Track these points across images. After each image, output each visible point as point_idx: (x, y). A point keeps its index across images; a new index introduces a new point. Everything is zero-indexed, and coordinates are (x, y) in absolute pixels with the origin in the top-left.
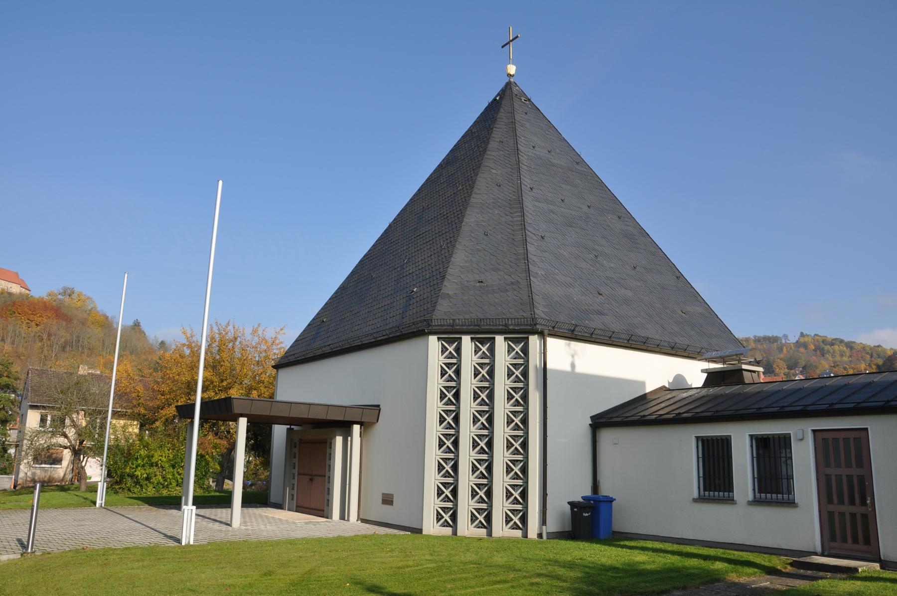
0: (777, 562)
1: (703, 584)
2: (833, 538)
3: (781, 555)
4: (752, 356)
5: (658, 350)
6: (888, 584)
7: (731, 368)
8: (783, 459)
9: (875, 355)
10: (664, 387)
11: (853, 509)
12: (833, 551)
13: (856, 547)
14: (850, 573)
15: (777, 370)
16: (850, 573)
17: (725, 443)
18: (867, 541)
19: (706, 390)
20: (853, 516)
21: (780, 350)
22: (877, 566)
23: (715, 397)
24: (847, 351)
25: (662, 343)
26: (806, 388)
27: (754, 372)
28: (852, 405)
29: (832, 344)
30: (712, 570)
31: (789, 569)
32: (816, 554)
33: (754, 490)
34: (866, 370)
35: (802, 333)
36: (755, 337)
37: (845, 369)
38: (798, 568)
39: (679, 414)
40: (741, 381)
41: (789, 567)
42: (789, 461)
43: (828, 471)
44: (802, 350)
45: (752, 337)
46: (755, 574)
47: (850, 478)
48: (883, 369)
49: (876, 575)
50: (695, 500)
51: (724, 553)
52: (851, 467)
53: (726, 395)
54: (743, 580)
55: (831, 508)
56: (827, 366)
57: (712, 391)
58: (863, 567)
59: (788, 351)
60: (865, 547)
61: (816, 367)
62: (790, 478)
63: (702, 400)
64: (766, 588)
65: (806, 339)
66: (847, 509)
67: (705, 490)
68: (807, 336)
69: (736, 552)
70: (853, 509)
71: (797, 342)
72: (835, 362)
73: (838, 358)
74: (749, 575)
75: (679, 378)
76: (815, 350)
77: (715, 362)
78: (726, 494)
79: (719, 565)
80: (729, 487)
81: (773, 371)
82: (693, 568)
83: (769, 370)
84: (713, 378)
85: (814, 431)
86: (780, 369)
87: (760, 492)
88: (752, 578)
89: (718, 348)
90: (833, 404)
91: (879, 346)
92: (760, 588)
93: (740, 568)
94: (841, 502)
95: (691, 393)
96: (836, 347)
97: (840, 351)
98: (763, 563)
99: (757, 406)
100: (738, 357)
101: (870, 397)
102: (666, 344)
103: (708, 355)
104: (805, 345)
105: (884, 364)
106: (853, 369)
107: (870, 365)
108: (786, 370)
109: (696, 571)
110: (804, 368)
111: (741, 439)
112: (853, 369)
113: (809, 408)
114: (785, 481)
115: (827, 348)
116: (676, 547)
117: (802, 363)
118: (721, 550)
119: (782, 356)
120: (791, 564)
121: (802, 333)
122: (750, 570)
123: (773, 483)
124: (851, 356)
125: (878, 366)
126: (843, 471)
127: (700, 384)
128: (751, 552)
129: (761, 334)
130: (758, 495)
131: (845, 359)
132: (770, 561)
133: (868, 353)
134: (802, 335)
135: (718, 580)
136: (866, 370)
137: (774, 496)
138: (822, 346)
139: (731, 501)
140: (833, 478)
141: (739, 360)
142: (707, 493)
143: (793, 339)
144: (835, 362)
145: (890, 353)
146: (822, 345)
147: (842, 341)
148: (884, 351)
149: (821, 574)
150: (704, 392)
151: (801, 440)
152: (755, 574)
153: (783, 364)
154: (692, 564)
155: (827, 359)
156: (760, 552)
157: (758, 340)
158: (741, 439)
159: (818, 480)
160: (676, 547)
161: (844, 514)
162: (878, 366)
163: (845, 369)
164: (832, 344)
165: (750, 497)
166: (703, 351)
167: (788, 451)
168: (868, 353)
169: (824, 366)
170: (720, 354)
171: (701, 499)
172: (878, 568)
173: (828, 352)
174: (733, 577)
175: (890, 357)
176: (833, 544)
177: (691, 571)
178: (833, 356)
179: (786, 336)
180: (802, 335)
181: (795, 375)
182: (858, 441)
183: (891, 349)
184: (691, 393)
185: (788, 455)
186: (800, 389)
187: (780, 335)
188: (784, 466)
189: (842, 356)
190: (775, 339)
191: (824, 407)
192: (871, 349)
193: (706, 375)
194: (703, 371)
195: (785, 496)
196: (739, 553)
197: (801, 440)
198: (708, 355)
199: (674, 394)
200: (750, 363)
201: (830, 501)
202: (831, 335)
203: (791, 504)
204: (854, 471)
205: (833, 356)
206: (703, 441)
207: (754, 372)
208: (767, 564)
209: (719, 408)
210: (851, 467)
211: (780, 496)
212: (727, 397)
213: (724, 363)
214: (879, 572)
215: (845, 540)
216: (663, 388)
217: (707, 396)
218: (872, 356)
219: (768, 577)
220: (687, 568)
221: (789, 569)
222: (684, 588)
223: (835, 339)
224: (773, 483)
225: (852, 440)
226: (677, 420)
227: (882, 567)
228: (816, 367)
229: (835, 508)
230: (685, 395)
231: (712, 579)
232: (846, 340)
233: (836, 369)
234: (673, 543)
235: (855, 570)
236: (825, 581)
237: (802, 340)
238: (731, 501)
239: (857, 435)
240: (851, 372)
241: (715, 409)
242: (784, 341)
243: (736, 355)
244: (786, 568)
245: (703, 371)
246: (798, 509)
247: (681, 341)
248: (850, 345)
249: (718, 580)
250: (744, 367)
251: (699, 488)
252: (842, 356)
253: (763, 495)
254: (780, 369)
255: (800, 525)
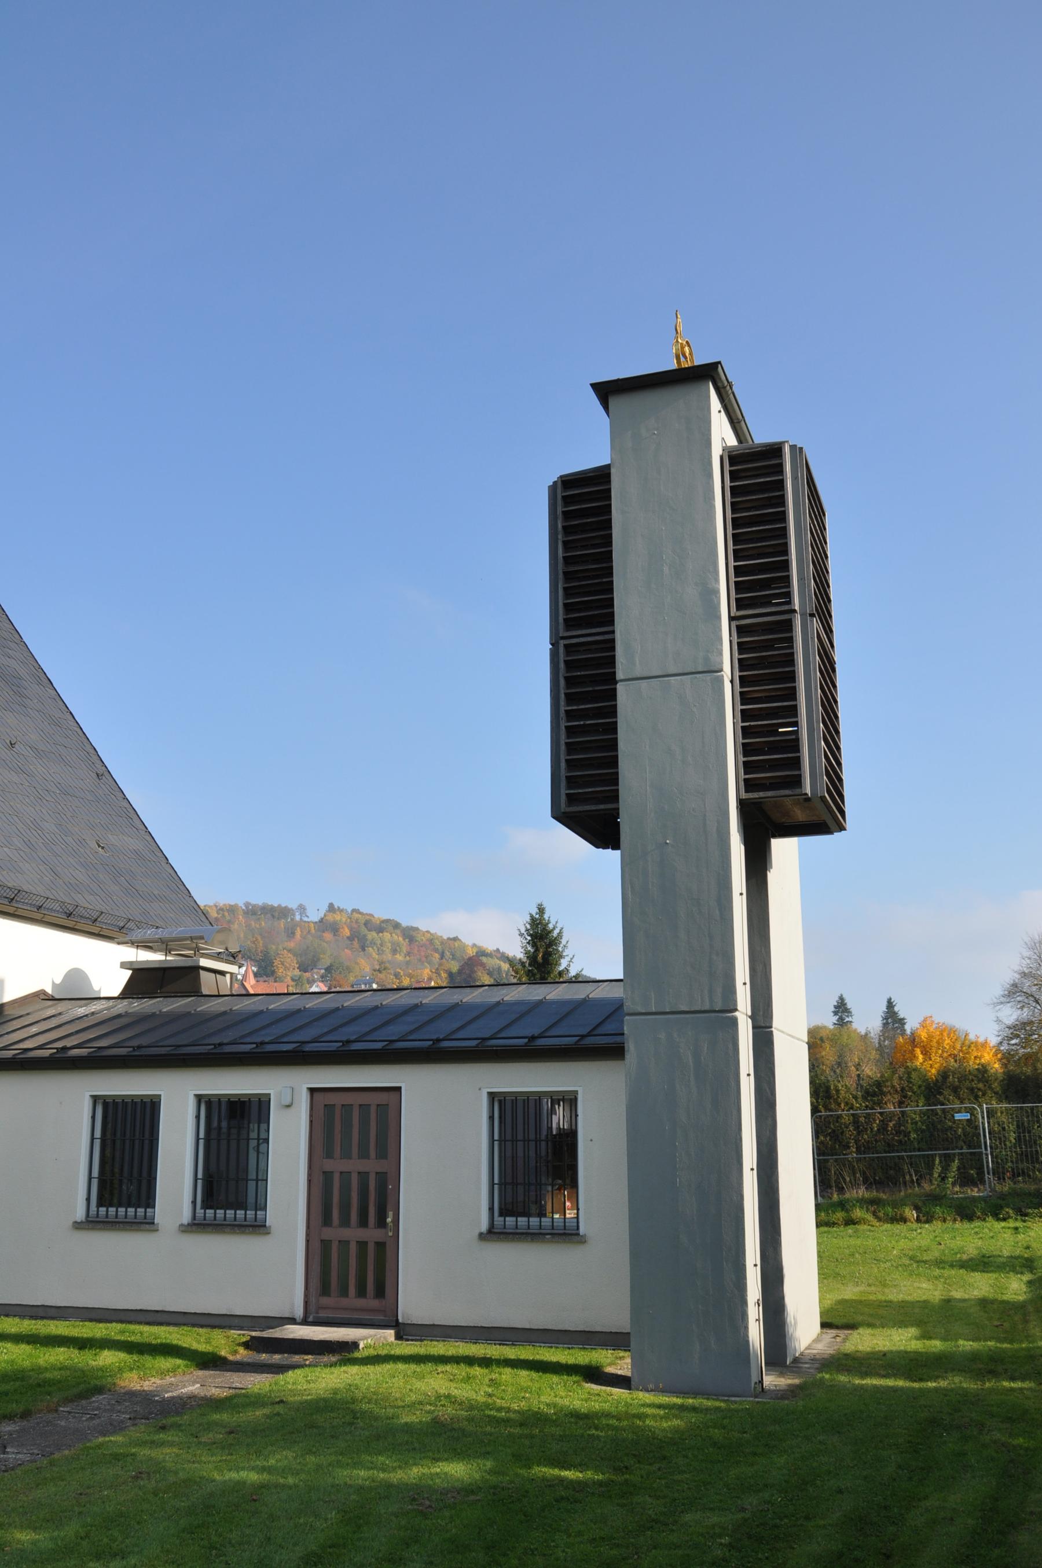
0: (222, 1343)
1: (67, 1401)
2: (325, 1290)
3: (230, 1327)
4: (222, 943)
5: (38, 916)
6: (401, 1366)
7: (181, 962)
8: (253, 1144)
9: (448, 954)
10: (43, 992)
11: (362, 1234)
12: (323, 1314)
13: (361, 1302)
14: (344, 1351)
15: (280, 972)
16: (344, 1351)
17: (147, 1111)
18: (380, 1292)
19: (125, 1002)
20: (362, 1245)
21: (291, 934)
22: (390, 1334)
23: (143, 1018)
24: (404, 944)
25: (48, 904)
26: (348, 1008)
27: (222, 973)
28: (379, 1046)
29: (380, 930)
30: (92, 1369)
31: (243, 1354)
32: (292, 1321)
33: (194, 1202)
34: (430, 979)
35: (331, 906)
36: (247, 904)
37: (397, 975)
38: (259, 1351)
39: (65, 1049)
40: (194, 990)
41: (241, 1350)
42: (263, 1147)
43: (329, 1165)
44: (328, 936)
45: (241, 904)
46: (174, 1370)
47: (363, 1176)
48: (458, 980)
49: (383, 1352)
50: (78, 1226)
51: (122, 1332)
52: (368, 1157)
53: (162, 1014)
54: (148, 1385)
55: (328, 1233)
56: (368, 969)
57: (137, 1006)
58: (370, 1339)
59: (304, 937)
60: (374, 1303)
61: (349, 970)
62: (262, 1180)
63: (115, 1023)
64: (192, 1397)
65: (338, 917)
66: (354, 1234)
67: (100, 1204)
68: (341, 911)
69: (146, 1329)
70: (362, 1234)
71: (321, 920)
72: (381, 963)
73: (388, 956)
74: (163, 1373)
75: (76, 976)
76: (351, 939)
77: (149, 948)
78: (141, 1211)
79: (108, 1358)
80: (147, 1198)
81: (273, 973)
82: (53, 1368)
83: (266, 969)
84: (143, 981)
85: (312, 1091)
86: (286, 969)
87: (206, 1206)
88: (169, 1379)
89: (160, 923)
90: (348, 1042)
91: (455, 939)
92: (180, 1398)
93: (148, 1360)
94: (363, 1222)
95: (95, 1007)
96: (387, 936)
97: (393, 943)
98: (195, 1346)
99: (216, 1040)
100: (195, 943)
101: (453, 1032)
102: (57, 907)
103: (138, 935)
104: (335, 929)
105: (460, 972)
106: (410, 976)
107: (437, 972)
108: (297, 972)
109: (57, 1375)
110: (328, 969)
111: (179, 1101)
112: (410, 976)
113: (308, 1048)
114: (252, 1185)
115: (372, 935)
116: (27, 1326)
117: (326, 961)
118: (119, 1326)
119: (291, 945)
120: (246, 1345)
121: (331, 906)
122: (166, 1363)
123: (229, 1190)
124: (408, 954)
125: (451, 975)
126: (355, 1165)
127: (116, 993)
128: (175, 1325)
129: (258, 900)
130: (200, 1212)
131: (399, 957)
132: (208, 1341)
133: (436, 950)
134: (331, 908)
135: (99, 1390)
136: (430, 979)
137: (230, 1213)
138: (363, 931)
139: (148, 1224)
140: (336, 1177)
141: (197, 949)
142: (103, 1210)
143: (314, 915)
144: (381, 963)
145: (471, 952)
146: (364, 930)
147: (397, 926)
148: (464, 947)
149: (297, 1358)
150: (122, 1007)
151: (288, 1106)
152: (174, 1370)
153: (291, 961)
154: (52, 1359)
155: (369, 956)
156: (194, 1325)
157: (253, 911)
158: (179, 1101)
159: (309, 1181)
160: (27, 1326)
161: (365, 1243)
162: (451, 975)
163: (397, 975)
164: (380, 930)
165: (186, 1217)
166: (131, 925)
167: (263, 1126)
168: (436, 950)
169: (362, 970)
170: (160, 934)
171: (91, 1223)
172: (392, 1339)
173: (373, 943)
174: (132, 1381)
175: (470, 959)
176: (325, 1301)
177: (48, 1375)
178: (380, 952)
179: (302, 908)
180: (331, 908)
181: (311, 982)
182: (382, 1108)
183: (474, 945)
184: (95, 1007)
185: (263, 1136)
186: (299, 1011)
187: (293, 905)
188: (252, 1155)
189: (394, 951)
190: (282, 913)
191: (334, 1046)
192: (442, 943)
193: (130, 972)
194: (124, 965)
195: (250, 1213)
196: (145, 1328)
197: (288, 1106)
198: (138, 935)
199: (60, 1007)
200: (218, 957)
201: (327, 1221)
202: (380, 913)
203: (259, 1227)
204: (372, 1166)
205: (380, 952)
206: (106, 1105)
207: (228, 976)
208: (202, 1347)
209: (143, 1041)
210: (368, 1157)
211: (240, 1213)
212: (168, 1018)
213: (168, 951)
214: (391, 1345)
215: (362, 1292)
216: (41, 996)
217: (127, 1014)
218: (442, 957)
219: (201, 1373)
220: (39, 1370)
221: (243, 1354)
222: (26, 1415)
223: (387, 921)
224: (229, 1190)
225: (373, 1109)
226: (60, 1062)
227: (399, 1337)
228: (349, 970)
229: (335, 1233)
230: (82, 1011)
231: (87, 1388)
232: (405, 923)
233: (382, 976)
234: (22, 1317)
235: (355, 1345)
236: (298, 1371)
237: (330, 918)
238: (148, 1224)
239: (373, 1099)
240: (406, 982)
241: (135, 1043)
242: (298, 918)
243: (192, 939)
244: (236, 1352)
245: (124, 965)
246: (267, 1238)
247: (89, 903)
248: (410, 934)
249: (99, 1390)
250: (204, 962)
251: (88, 1200)
252: (394, 951)
253: (210, 1212)
254: (286, 969)
255: (268, 1270)
